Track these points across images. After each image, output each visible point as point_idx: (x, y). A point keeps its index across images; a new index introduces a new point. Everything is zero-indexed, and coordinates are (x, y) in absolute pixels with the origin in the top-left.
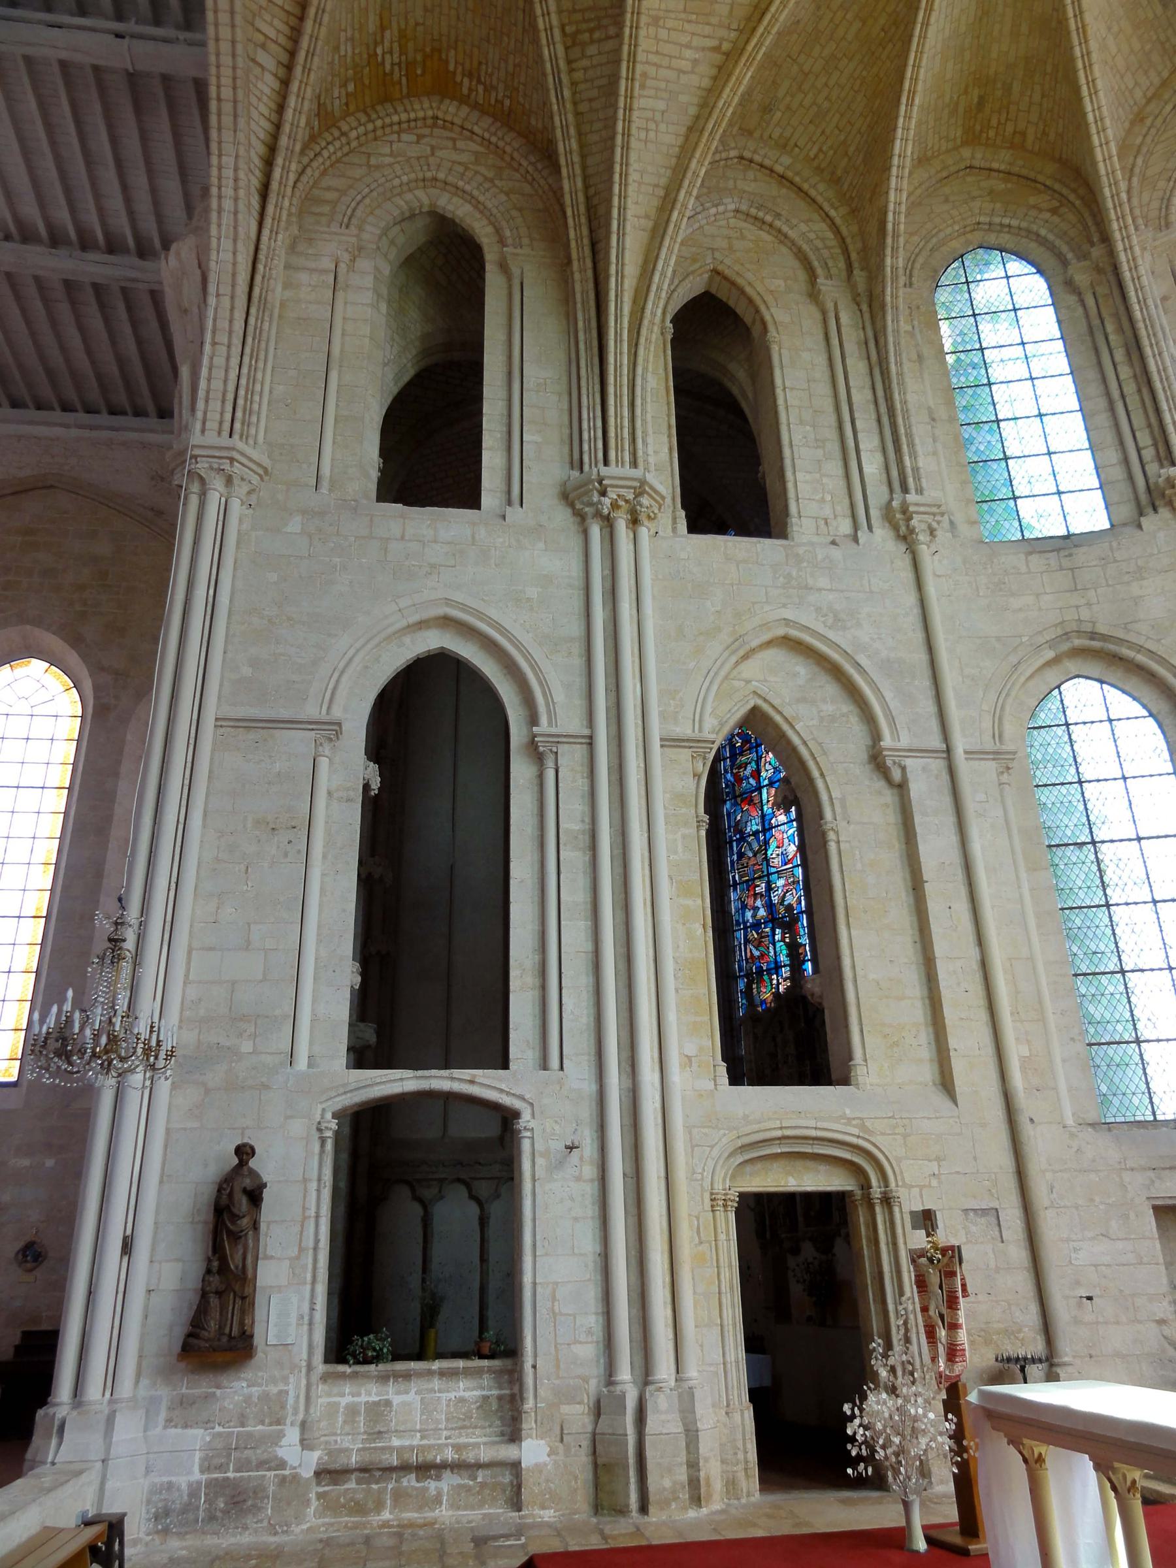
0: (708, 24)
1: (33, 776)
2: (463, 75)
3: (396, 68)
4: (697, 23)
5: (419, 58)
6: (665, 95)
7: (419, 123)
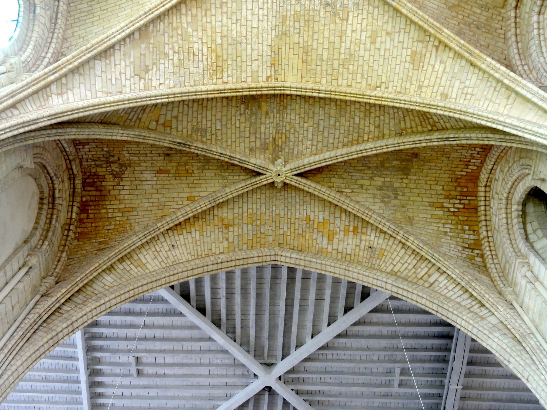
0: (425, 55)
2: (467, 168)
3: (462, 202)
4: (424, 62)
5: (459, 189)
6: (453, 80)
7: (488, 195)
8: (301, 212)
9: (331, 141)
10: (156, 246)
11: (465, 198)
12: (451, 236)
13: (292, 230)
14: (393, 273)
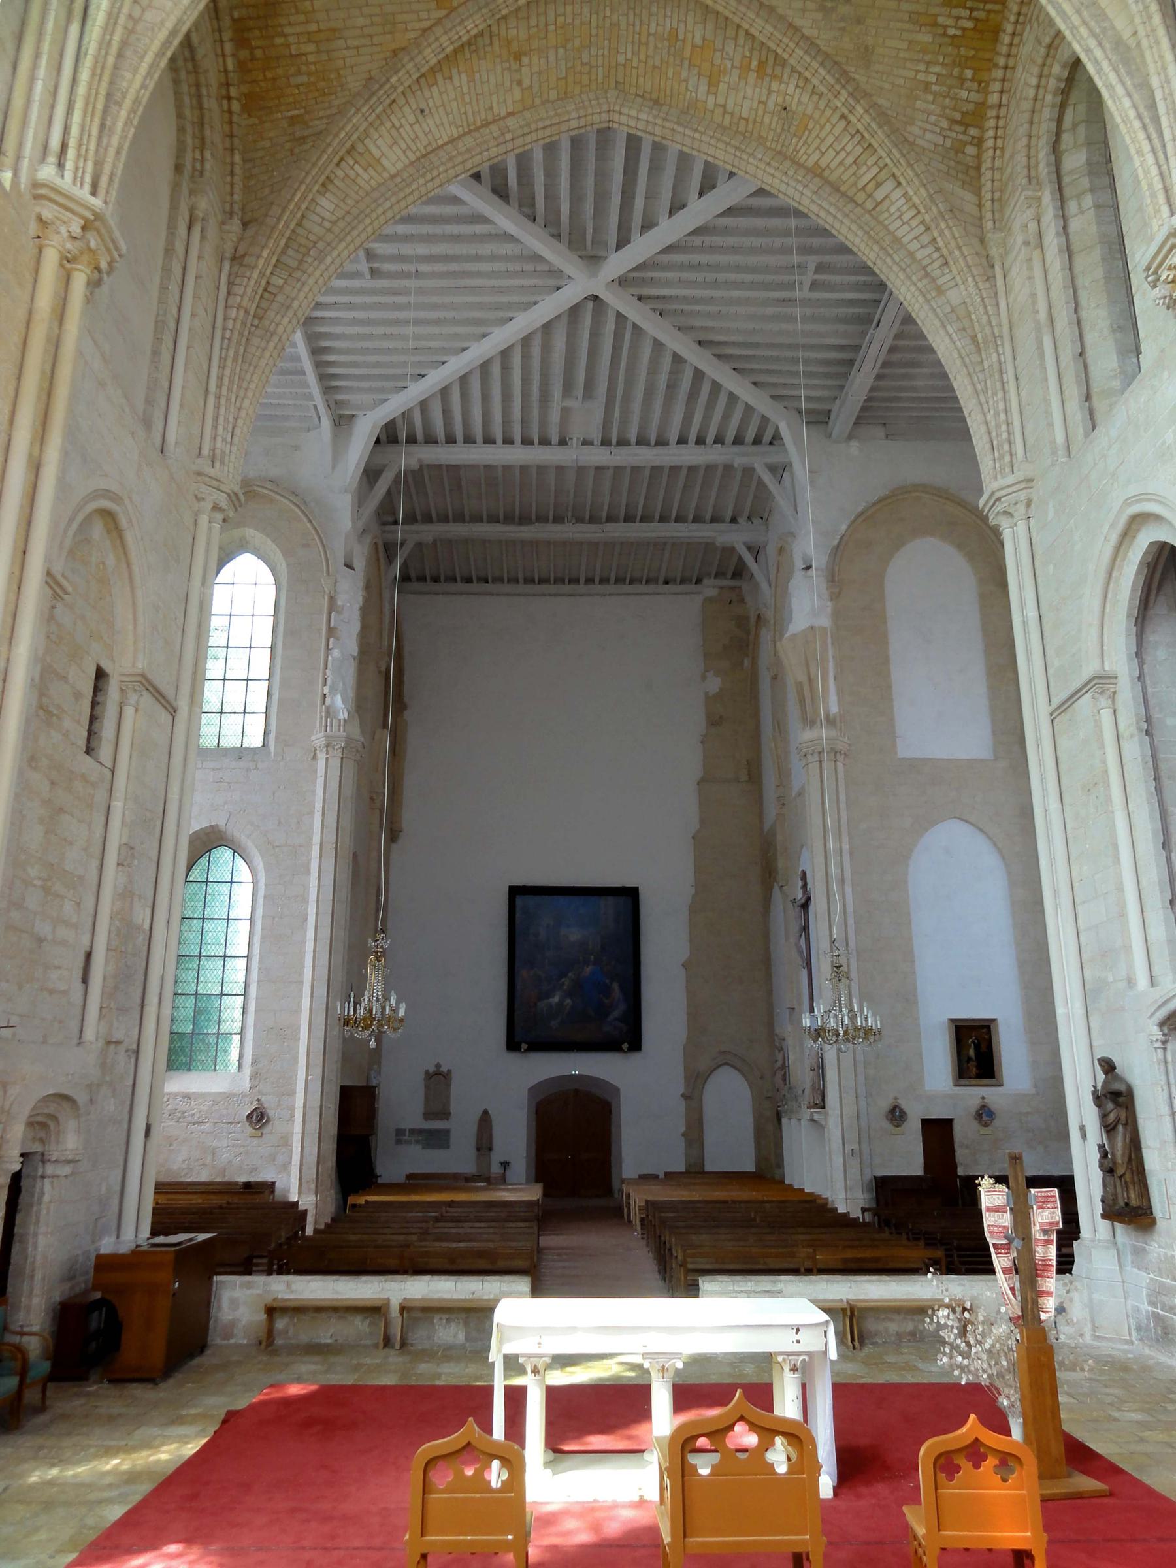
8: (661, 22)
10: (392, 117)
11: (981, 6)
12: (935, 94)
13: (642, 57)
14: (816, 172)
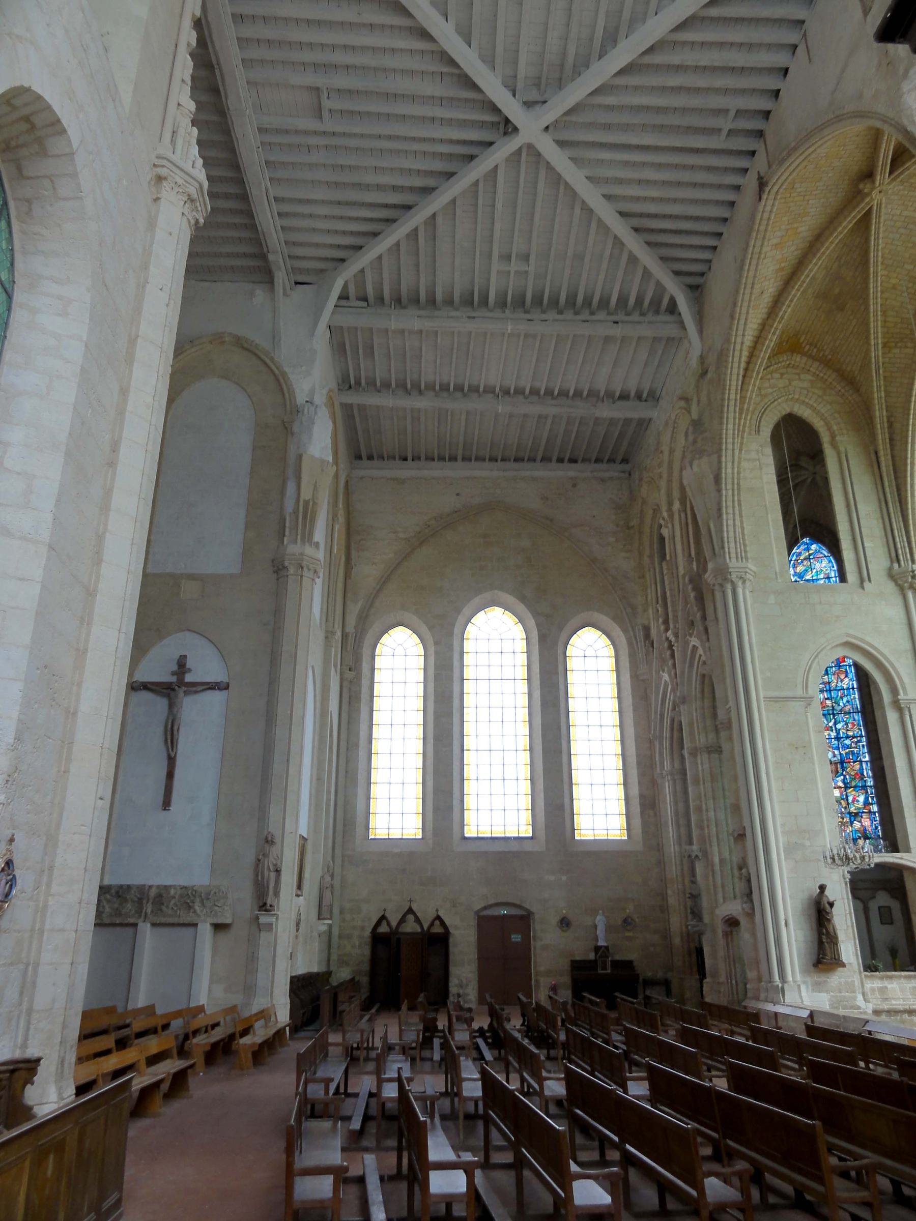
1: (508, 673)
2: (807, 344)
9: (891, 236)
